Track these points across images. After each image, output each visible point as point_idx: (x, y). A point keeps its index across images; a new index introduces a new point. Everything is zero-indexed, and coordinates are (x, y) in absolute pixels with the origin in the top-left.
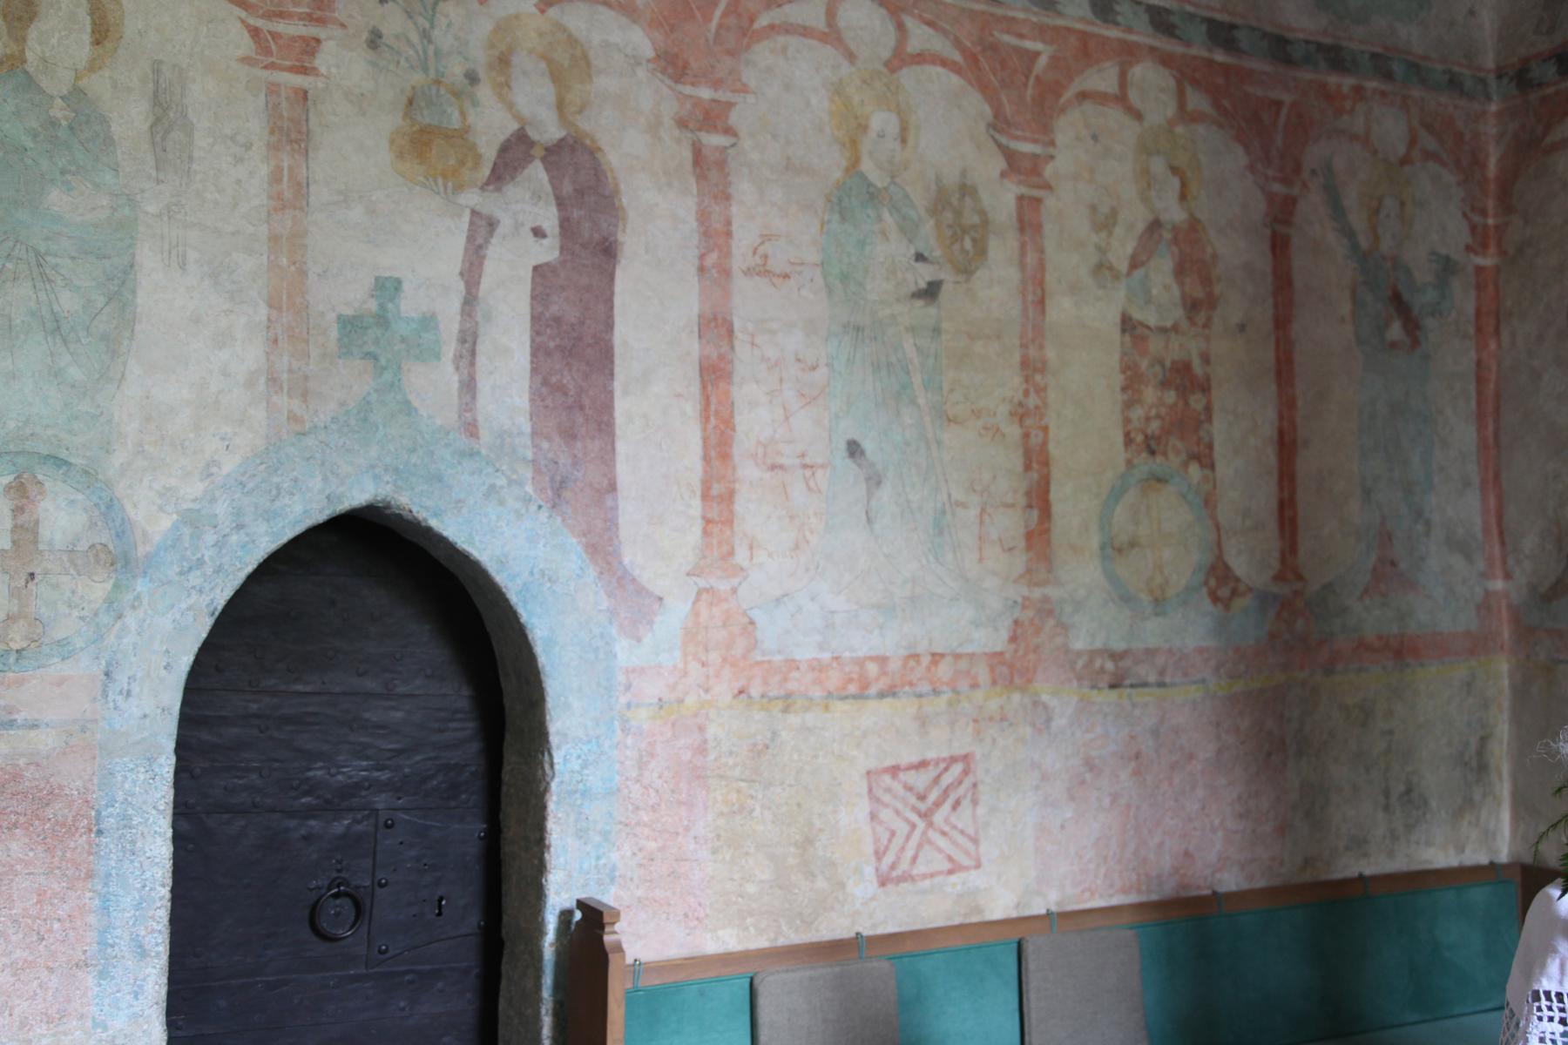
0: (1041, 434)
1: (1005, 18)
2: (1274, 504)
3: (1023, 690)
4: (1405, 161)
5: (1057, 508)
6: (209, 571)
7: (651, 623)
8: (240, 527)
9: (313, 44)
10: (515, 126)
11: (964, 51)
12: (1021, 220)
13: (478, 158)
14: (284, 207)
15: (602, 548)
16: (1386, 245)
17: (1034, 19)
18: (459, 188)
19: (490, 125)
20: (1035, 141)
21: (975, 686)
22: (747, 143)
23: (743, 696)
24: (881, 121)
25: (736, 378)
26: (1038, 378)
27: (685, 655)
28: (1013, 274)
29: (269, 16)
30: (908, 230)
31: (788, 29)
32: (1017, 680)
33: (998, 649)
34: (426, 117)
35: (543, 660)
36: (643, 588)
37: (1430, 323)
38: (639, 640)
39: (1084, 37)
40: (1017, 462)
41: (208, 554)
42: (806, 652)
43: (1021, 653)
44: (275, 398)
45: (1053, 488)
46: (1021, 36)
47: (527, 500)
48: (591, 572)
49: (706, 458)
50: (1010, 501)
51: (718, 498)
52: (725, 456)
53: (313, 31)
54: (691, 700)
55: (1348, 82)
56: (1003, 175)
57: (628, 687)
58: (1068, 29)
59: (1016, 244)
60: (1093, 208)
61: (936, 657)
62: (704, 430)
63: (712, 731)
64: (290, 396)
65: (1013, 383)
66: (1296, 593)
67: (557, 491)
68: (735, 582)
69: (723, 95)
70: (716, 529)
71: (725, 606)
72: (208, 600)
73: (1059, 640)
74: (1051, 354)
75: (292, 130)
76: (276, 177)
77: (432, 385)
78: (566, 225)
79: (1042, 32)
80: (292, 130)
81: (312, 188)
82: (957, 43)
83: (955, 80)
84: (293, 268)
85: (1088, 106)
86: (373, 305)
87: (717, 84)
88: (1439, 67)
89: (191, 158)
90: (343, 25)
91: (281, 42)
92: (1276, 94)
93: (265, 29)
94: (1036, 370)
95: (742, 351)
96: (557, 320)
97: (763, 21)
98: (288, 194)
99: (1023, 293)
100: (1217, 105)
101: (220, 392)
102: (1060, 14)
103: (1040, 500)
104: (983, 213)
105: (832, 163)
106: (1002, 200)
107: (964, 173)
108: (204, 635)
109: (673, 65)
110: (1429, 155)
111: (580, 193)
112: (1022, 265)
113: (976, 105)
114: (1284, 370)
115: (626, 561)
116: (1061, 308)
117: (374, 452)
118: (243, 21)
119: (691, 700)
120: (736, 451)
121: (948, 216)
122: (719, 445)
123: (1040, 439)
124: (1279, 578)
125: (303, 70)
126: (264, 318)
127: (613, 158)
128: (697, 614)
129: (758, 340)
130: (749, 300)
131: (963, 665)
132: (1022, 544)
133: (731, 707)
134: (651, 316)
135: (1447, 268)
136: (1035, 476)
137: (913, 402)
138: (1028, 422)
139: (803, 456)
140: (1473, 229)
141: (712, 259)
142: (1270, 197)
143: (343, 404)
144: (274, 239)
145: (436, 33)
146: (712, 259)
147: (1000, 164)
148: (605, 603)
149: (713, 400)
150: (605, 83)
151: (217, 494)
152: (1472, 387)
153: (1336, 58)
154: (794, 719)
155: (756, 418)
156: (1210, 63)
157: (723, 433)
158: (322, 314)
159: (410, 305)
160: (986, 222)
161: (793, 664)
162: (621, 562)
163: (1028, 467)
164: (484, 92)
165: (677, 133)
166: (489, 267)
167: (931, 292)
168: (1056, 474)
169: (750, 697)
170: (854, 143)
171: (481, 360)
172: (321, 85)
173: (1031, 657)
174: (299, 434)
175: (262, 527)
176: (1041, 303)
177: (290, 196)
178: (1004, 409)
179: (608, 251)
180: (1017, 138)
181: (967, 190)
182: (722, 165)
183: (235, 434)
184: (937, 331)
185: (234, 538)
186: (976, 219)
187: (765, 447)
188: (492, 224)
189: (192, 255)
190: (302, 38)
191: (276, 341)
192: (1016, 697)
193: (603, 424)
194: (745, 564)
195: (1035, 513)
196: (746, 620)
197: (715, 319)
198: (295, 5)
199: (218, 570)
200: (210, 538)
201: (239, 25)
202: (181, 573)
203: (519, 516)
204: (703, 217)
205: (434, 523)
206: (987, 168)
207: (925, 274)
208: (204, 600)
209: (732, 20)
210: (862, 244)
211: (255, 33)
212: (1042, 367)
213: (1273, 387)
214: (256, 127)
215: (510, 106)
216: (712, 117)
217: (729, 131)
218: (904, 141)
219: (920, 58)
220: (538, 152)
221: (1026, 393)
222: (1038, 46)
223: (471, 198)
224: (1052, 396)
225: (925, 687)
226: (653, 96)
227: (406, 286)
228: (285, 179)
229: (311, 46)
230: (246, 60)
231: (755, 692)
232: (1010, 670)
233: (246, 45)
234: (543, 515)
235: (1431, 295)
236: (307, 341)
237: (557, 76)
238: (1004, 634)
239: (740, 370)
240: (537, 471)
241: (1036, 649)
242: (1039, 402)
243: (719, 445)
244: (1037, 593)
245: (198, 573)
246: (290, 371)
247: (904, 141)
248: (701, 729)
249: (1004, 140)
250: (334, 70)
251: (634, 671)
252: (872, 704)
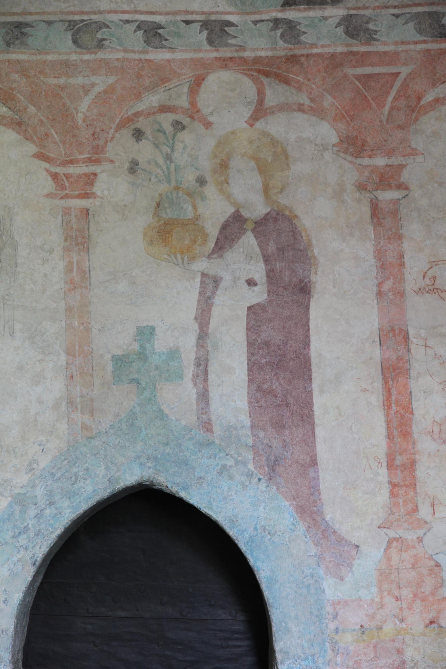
6: (32, 534)
7: (350, 565)
8: (51, 504)
9: (92, 177)
10: (231, 210)
13: (205, 236)
14: (75, 288)
15: (309, 509)
18: (192, 259)
19: (214, 211)
22: (416, 193)
23: (433, 625)
25: (413, 373)
27: (381, 590)
29: (64, 164)
34: (169, 214)
35: (267, 594)
36: (343, 538)
38: (342, 579)
41: (31, 523)
44: (73, 415)
47: (250, 475)
48: (301, 528)
49: (390, 437)
52: (406, 434)
53: (92, 168)
57: (335, 616)
62: (387, 415)
63: (409, 653)
64: (82, 413)
67: (272, 468)
68: (420, 533)
69: (395, 161)
70: (401, 492)
71: (413, 552)
72: (31, 554)
75: (79, 237)
76: (69, 269)
77: (178, 398)
78: (272, 276)
80: (79, 237)
81: (92, 273)
84: (82, 327)
86: (136, 346)
87: (389, 153)
89: (16, 264)
90: (112, 161)
91: (71, 180)
93: (61, 173)
95: (417, 352)
96: (267, 344)
97: (429, 97)
98: (77, 279)
101: (38, 414)
108: (30, 579)
109: (353, 145)
111: (281, 250)
115: (328, 518)
117: (139, 447)
118: (47, 170)
119: (388, 628)
120: (415, 429)
122: (400, 426)
125: (86, 196)
126: (65, 362)
127: (306, 222)
128: (389, 559)
129: (430, 343)
133: (424, 635)
134: (340, 334)
143: (117, 415)
144: (69, 309)
145: (176, 155)
148: (313, 551)
149: (394, 391)
150: (300, 168)
151: (37, 482)
157: (402, 416)
158: (102, 356)
159: (161, 344)
162: (324, 519)
164: (210, 190)
165: (357, 195)
166: (216, 311)
169: (441, 627)
171: (212, 377)
172: (97, 204)
174: (89, 438)
175: (66, 503)
177: (79, 280)
179: (304, 289)
182: (395, 214)
183: (48, 441)
185: (48, 512)
187: (441, 425)
188: (217, 281)
189: (18, 326)
190: (85, 174)
191: (72, 377)
193: (305, 415)
194: (429, 518)
196: (433, 563)
197: (393, 330)
198: (80, 153)
199: (37, 534)
200: (32, 512)
201: (45, 173)
202: (14, 537)
203: (244, 487)
204: (379, 254)
205: (183, 495)
208: (29, 555)
209: (402, 102)
211: (55, 176)
214: (56, 238)
215: (229, 197)
216: (388, 178)
217: (401, 186)
220: (249, 225)
223: (202, 265)
226: (340, 171)
227: (158, 331)
228: (75, 269)
229: (91, 178)
230: (50, 196)
233: (49, 185)
234: (263, 486)
236: (92, 375)
237: (263, 169)
239: (416, 367)
240: (256, 454)
243: (400, 426)
245: (25, 536)
246: (82, 396)
248: (399, 652)
250: (106, 192)
251: (339, 603)
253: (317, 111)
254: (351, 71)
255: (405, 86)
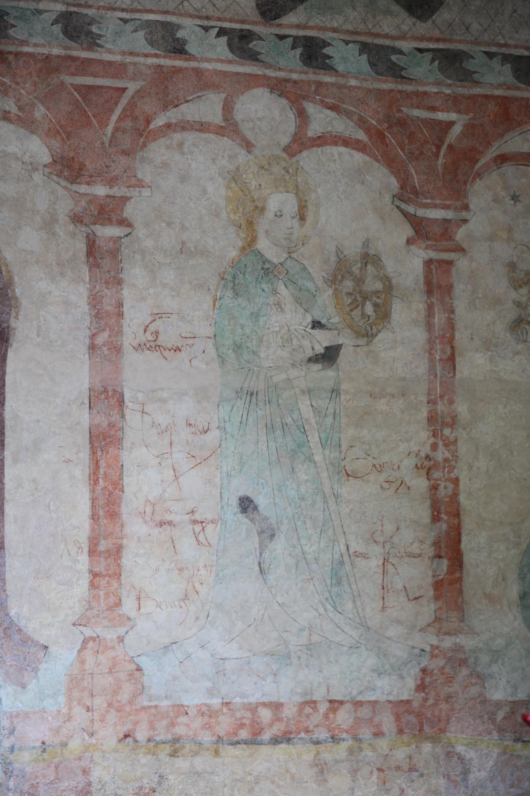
0: (451, 486)
1: (417, 94)
3: (434, 740)
5: (469, 558)
7: (36, 670)
11: (368, 131)
12: (428, 283)
17: (448, 91)
20: (446, 207)
21: (378, 734)
22: (141, 232)
23: (128, 740)
24: (280, 201)
25: (126, 443)
26: (447, 432)
27: (70, 699)
28: (420, 335)
30: (304, 299)
31: (184, 126)
32: (427, 729)
33: (405, 697)
36: (29, 638)
38: (24, 687)
39: (504, 102)
40: (424, 513)
42: (193, 699)
43: (431, 702)
45: (464, 539)
46: (433, 109)
49: (94, 517)
50: (418, 551)
51: (105, 554)
52: (114, 515)
54: (75, 744)
56: (409, 242)
57: (12, 732)
58: (486, 97)
59: (422, 306)
60: (512, 266)
61: (335, 705)
62: (93, 491)
63: (96, 774)
65: (420, 438)
68: (121, 631)
69: (117, 191)
70: (103, 582)
71: (111, 654)
73: (474, 690)
74: (462, 408)
79: (455, 103)
82: (362, 123)
83: (358, 157)
85: (509, 169)
87: (111, 182)
94: (444, 424)
95: (133, 418)
97: (160, 121)
99: (430, 352)
102: (477, 83)
103: (450, 549)
104: (387, 280)
105: (226, 244)
106: (408, 266)
107: (366, 243)
109: (69, 168)
112: (429, 326)
113: (382, 180)
115: (12, 613)
116: (473, 364)
119: (75, 744)
120: (124, 510)
121: (348, 284)
122: (107, 505)
123: (450, 491)
128: (83, 662)
129: (149, 408)
130: (138, 373)
131: (365, 712)
132: (431, 593)
133: (116, 751)
136: (444, 526)
137: (310, 459)
138: (436, 475)
139: (193, 512)
141: (102, 338)
146: (102, 338)
147: (408, 231)
149: (103, 464)
154: (182, 763)
155: (144, 479)
157: (111, 494)
160: (389, 287)
161: (181, 710)
162: (7, 615)
163: (435, 519)
165: (71, 227)
167: (329, 356)
168: (468, 524)
169: (136, 741)
170: (250, 223)
173: (443, 706)
176: (452, 359)
178: (409, 463)
180: (426, 206)
181: (369, 258)
182: (115, 254)
184: (335, 392)
186: (379, 286)
187: (154, 505)
192: (427, 747)
194: (133, 614)
195: (445, 563)
196: (134, 667)
197: (106, 391)
204: (95, 301)
206: (391, 238)
207: (322, 340)
209: (128, 124)
210: (255, 316)
212: (453, 422)
216: (108, 212)
217: (123, 222)
218: (302, 218)
219: (321, 141)
221: (434, 447)
222: (453, 116)
224: (463, 449)
225: (322, 734)
231: (141, 735)
232: (420, 718)
238: (411, 683)
239: (130, 436)
241: (448, 698)
242: (447, 455)
243: (107, 505)
244: (448, 642)
247: (302, 218)
248: (85, 772)
249: (411, 209)
251: (18, 715)
252: (265, 750)
253: (27, 123)
254: (69, 80)
255: (132, 105)
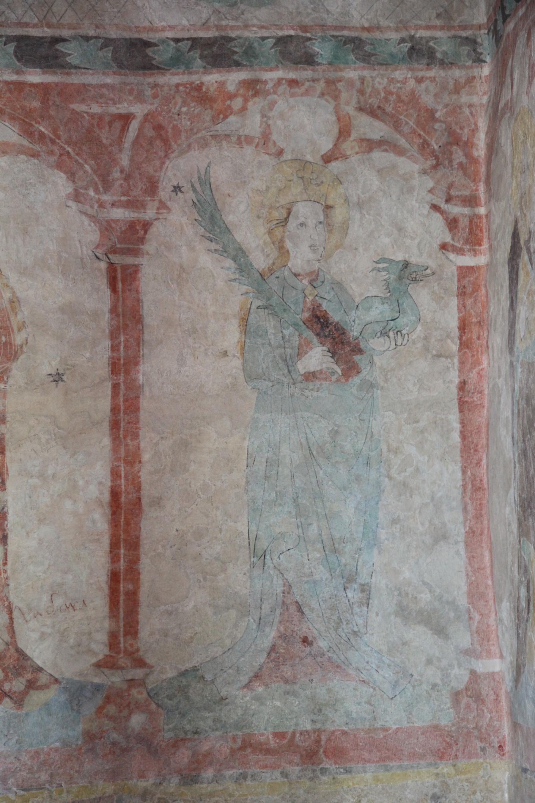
2: (102, 577)
4: (327, 159)
16: (301, 258)
37: (376, 344)
55: (233, 78)
66: (131, 682)
88: (394, 36)
92: (122, 108)
100: (27, 132)
110: (370, 145)
114: (124, 418)
124: (107, 664)
135: (407, 274)
140: (452, 224)
142: (106, 228)
152: (454, 418)
153: (219, 52)
156: (20, 86)
213: (107, 441)
235: (379, 311)
